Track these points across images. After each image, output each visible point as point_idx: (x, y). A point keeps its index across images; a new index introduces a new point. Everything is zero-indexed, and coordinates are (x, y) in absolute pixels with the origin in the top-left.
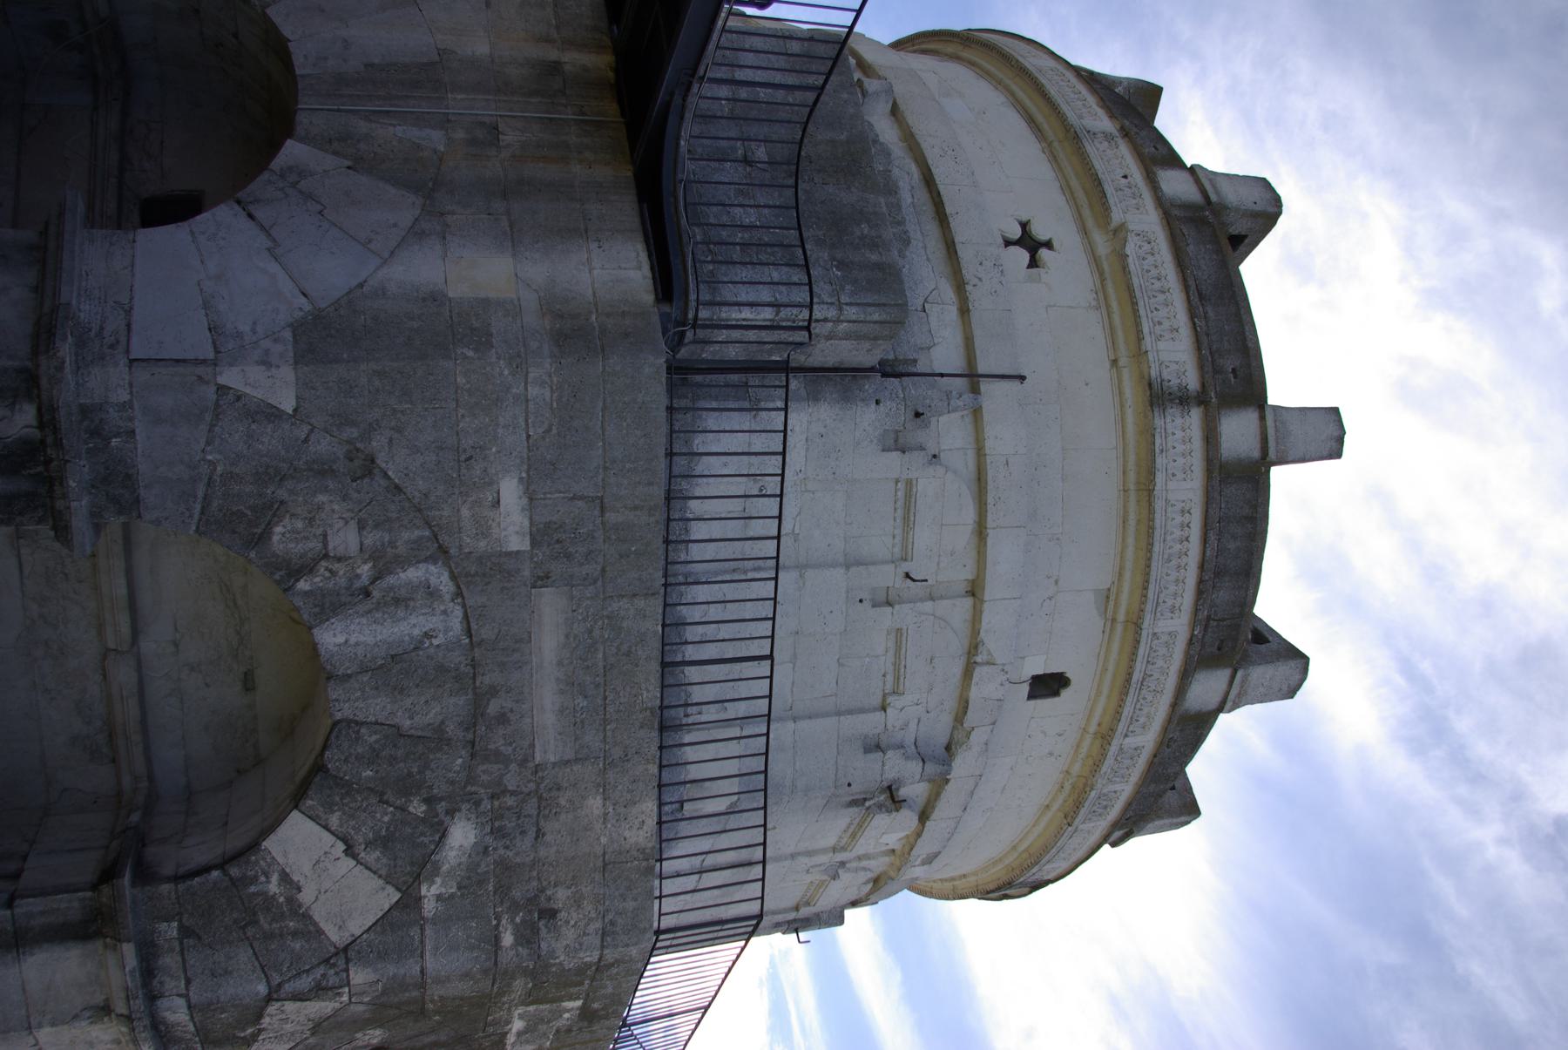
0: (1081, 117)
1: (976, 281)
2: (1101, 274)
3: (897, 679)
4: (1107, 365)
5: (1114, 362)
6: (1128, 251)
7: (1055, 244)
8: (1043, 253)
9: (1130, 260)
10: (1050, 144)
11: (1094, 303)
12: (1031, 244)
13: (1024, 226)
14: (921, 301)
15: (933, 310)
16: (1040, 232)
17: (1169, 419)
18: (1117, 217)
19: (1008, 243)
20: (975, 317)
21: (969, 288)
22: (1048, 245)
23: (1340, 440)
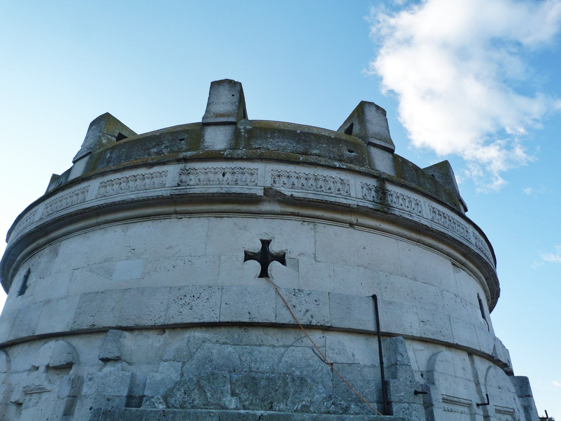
0: (164, 186)
1: (308, 315)
2: (293, 214)
3: (508, 413)
4: (351, 230)
5: (351, 225)
6: (288, 193)
7: (265, 238)
8: (274, 248)
9: (296, 195)
10: (176, 213)
11: (311, 226)
12: (265, 257)
13: (248, 256)
14: (323, 364)
15: (331, 357)
16: (257, 247)
17: (394, 205)
18: (260, 193)
19: (264, 274)
20: (336, 323)
21: (314, 322)
22: (266, 243)
23: (378, 108)
